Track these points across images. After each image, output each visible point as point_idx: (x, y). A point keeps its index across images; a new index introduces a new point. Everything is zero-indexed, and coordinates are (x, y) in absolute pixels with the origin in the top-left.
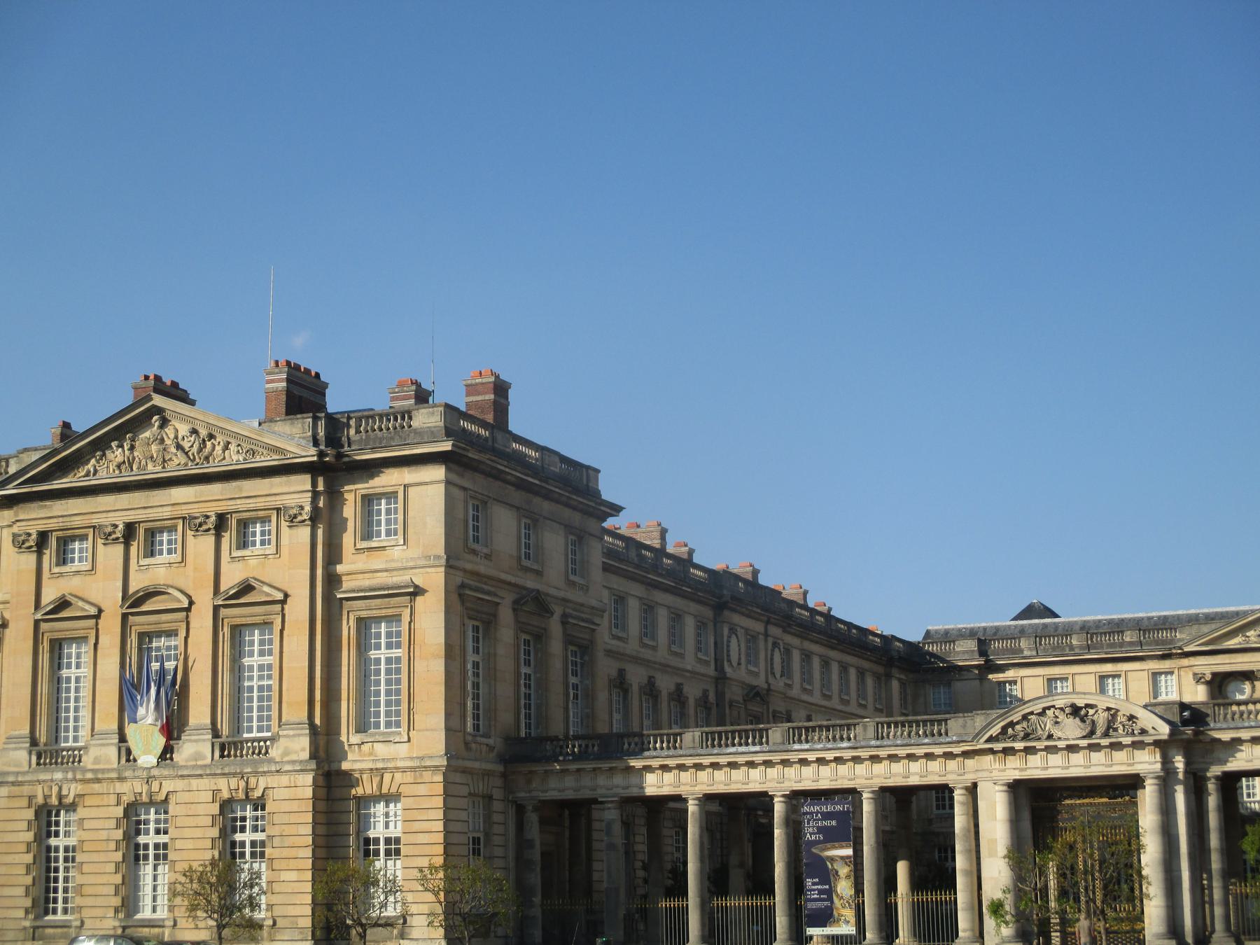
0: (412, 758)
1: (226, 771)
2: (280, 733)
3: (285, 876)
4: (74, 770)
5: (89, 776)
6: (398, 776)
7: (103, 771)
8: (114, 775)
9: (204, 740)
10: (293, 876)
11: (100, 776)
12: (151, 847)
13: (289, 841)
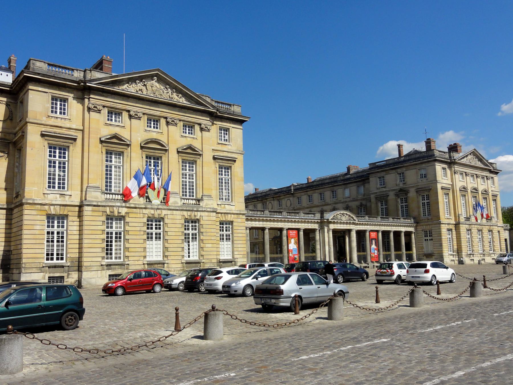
1: (188, 209)
3: (207, 245)
6: (232, 215)
7: (139, 204)
8: (143, 206)
10: (210, 245)
12: (191, 235)
13: (209, 234)
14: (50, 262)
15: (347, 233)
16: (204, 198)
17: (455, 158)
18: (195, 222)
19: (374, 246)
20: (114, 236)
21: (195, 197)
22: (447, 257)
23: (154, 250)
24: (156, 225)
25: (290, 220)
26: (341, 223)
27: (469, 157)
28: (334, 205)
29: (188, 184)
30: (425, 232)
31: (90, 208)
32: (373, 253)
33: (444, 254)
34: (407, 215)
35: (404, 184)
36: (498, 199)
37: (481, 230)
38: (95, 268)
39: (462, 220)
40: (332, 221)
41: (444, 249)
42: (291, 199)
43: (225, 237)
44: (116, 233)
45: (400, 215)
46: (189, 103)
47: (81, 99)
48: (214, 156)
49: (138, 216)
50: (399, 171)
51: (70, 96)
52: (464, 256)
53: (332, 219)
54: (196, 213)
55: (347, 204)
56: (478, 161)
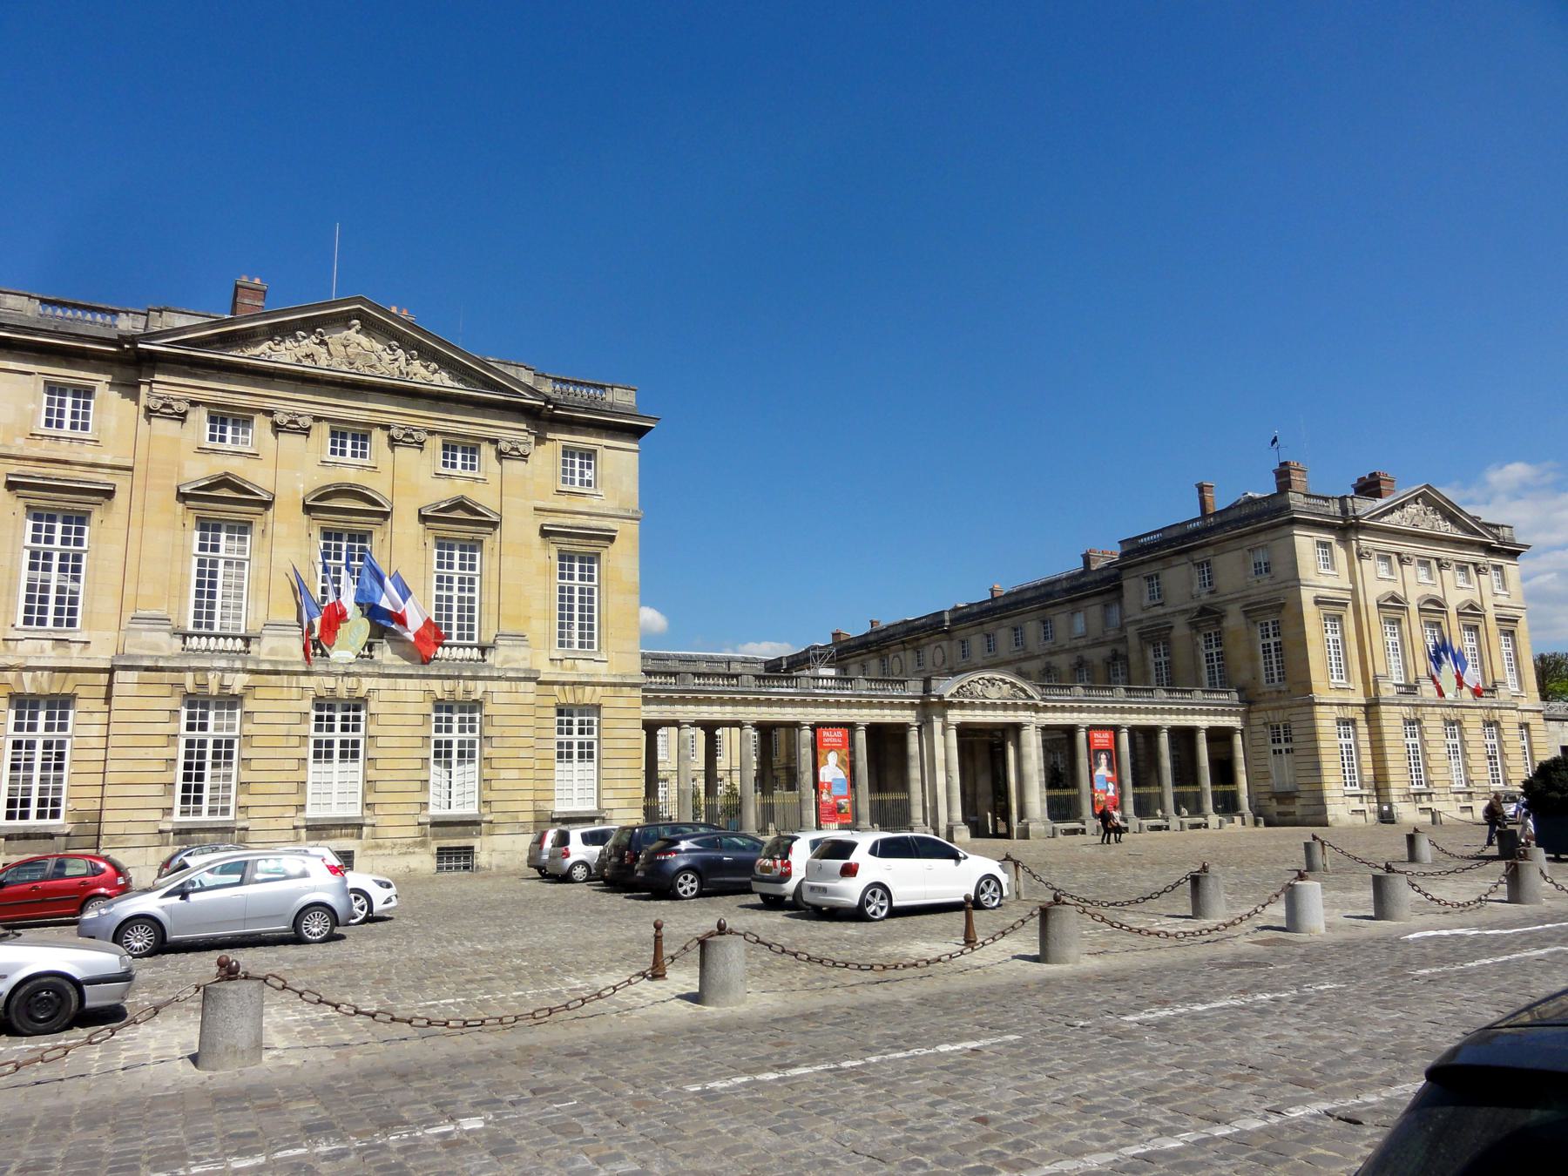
3: (504, 774)
4: (244, 660)
6: (599, 689)
7: (286, 663)
10: (514, 774)
14: (17, 822)
15: (1011, 734)
16: (499, 642)
17: (1357, 514)
18: (472, 710)
19: (1103, 771)
20: (209, 750)
21: (476, 641)
22: (1340, 800)
23: (335, 788)
24: (345, 718)
25: (820, 699)
26: (984, 707)
27: (1412, 509)
28: (1049, 659)
29: (455, 604)
30: (1272, 728)
31: (133, 676)
32: (1102, 791)
33: (1327, 793)
34: (1222, 679)
35: (1211, 592)
36: (1522, 629)
37: (1459, 722)
38: (139, 841)
39: (1387, 691)
40: (955, 700)
41: (1326, 779)
42: (944, 644)
43: (576, 750)
44: (217, 744)
45: (1153, 678)
46: (461, 386)
47: (129, 388)
48: (542, 526)
49: (285, 693)
50: (1198, 556)
51: (101, 382)
52: (1394, 799)
53: (952, 695)
54: (471, 684)
55: (1078, 654)
56: (1444, 520)
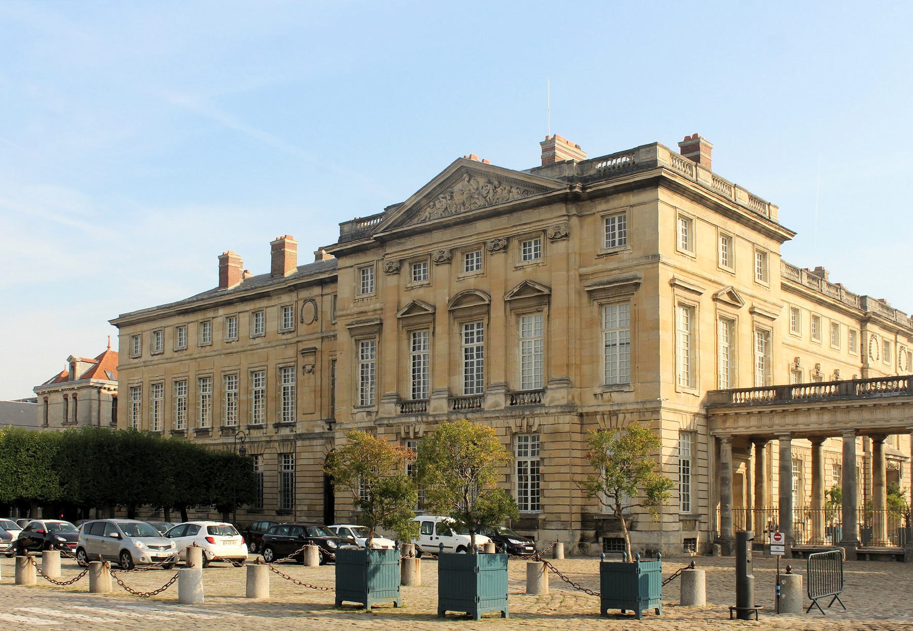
0: (637, 403)
2: (549, 387)
3: (553, 485)
5: (431, 419)
6: (628, 416)
9: (499, 393)
10: (557, 485)
11: (437, 419)
54: (531, 420)
